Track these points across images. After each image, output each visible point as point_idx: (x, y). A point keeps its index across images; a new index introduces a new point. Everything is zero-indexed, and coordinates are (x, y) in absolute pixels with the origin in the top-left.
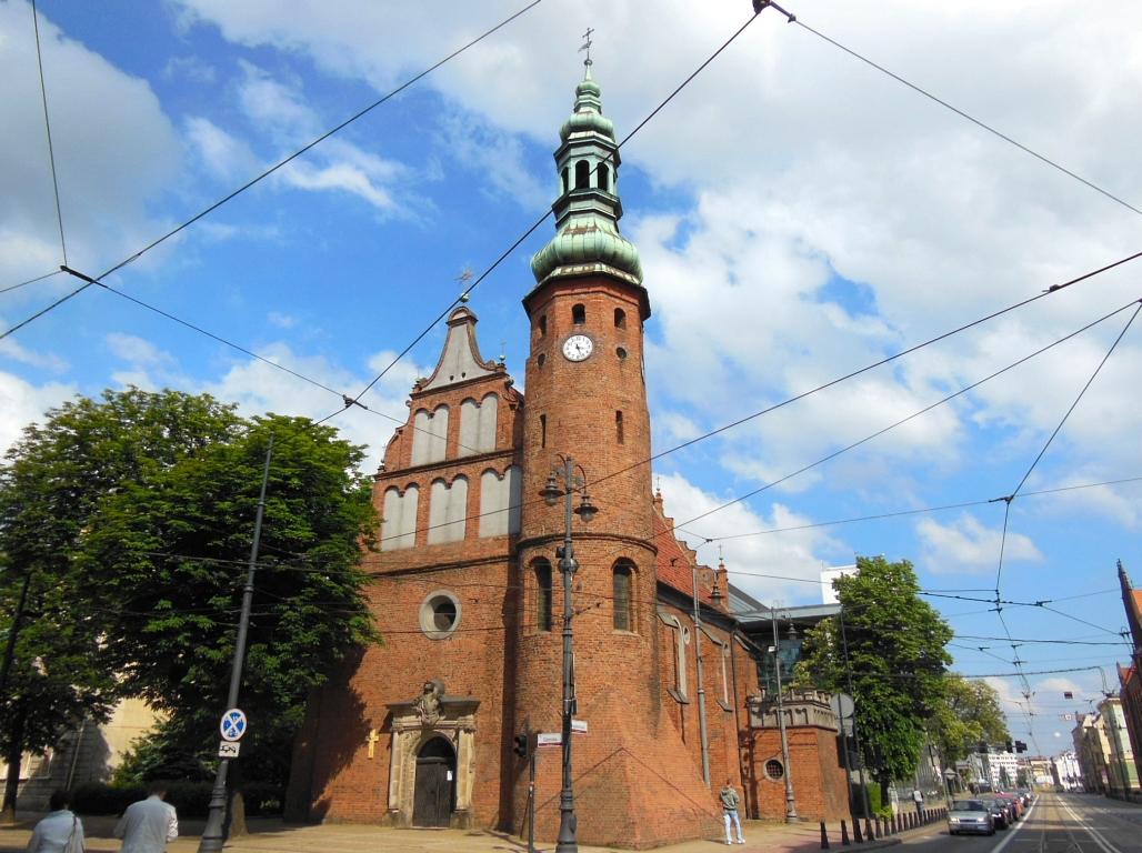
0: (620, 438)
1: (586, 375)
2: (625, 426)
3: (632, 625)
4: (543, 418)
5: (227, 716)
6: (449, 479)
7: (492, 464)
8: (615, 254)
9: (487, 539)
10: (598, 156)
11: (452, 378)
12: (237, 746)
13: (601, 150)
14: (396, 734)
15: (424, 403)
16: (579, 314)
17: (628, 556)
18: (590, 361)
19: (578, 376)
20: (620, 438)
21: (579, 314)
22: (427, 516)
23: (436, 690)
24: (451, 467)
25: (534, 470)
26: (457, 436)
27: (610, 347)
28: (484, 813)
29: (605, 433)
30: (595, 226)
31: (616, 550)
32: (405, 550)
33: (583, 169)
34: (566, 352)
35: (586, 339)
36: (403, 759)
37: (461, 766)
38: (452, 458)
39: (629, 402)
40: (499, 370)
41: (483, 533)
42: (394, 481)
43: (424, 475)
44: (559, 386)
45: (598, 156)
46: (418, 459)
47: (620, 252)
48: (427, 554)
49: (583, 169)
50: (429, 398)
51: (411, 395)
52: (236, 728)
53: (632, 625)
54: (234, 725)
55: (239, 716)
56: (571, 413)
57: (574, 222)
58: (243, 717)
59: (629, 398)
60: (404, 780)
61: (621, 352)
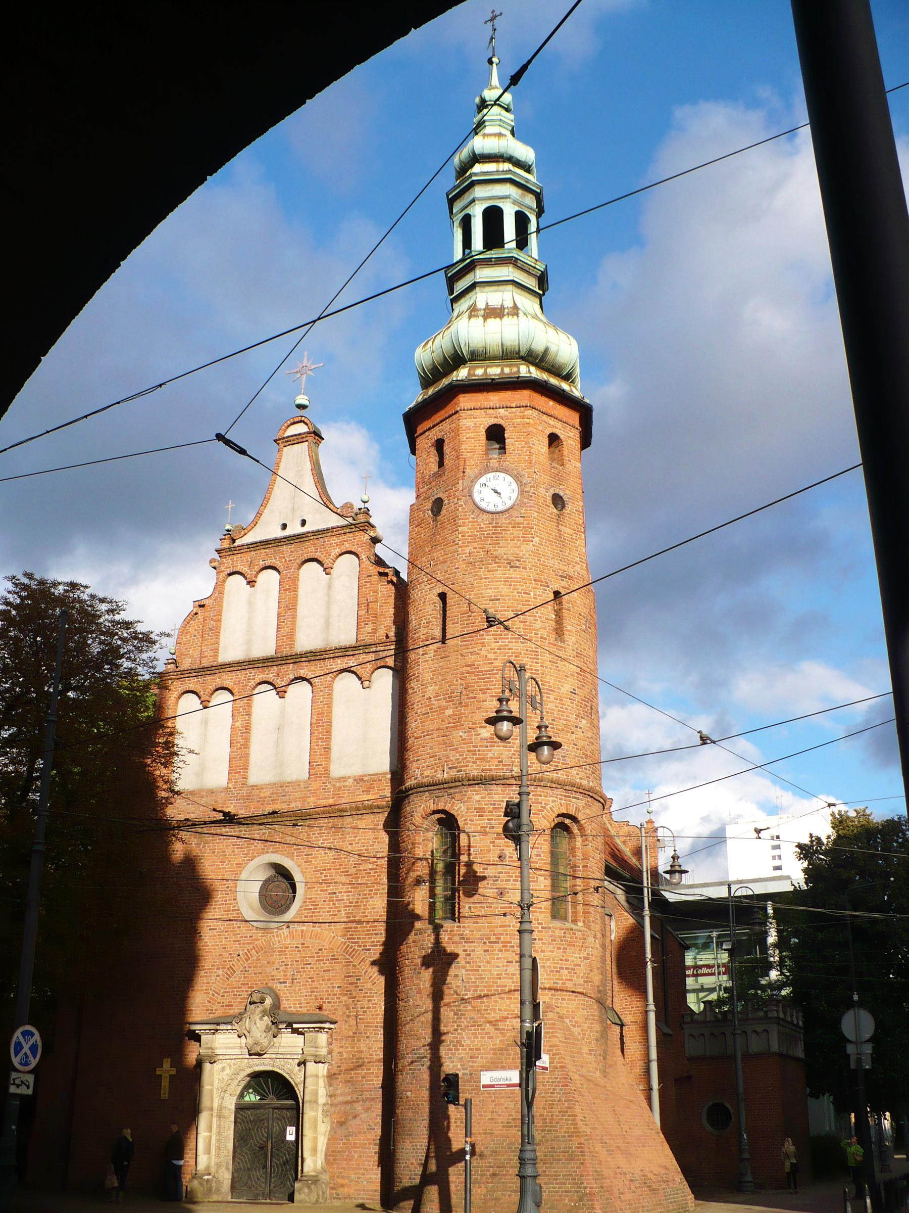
0: (559, 631)
2: (565, 613)
3: (575, 913)
4: (443, 596)
5: (18, 1034)
6: (279, 683)
8: (547, 350)
9: (343, 779)
10: (515, 202)
11: (284, 526)
13: (520, 191)
15: (240, 562)
16: (496, 434)
17: (572, 812)
18: (514, 513)
19: (496, 534)
22: (247, 740)
23: (268, 1001)
24: (285, 665)
25: (427, 677)
26: (294, 617)
28: (346, 1181)
29: (538, 625)
30: (515, 307)
32: (212, 792)
33: (493, 217)
34: (477, 497)
35: (509, 479)
37: (310, 1115)
38: (286, 651)
39: (570, 578)
40: (362, 519)
41: (336, 770)
42: (191, 684)
43: (241, 675)
44: (467, 550)
46: (230, 651)
47: (553, 349)
48: (248, 797)
49: (493, 217)
51: (218, 551)
52: (29, 1053)
53: (575, 913)
54: (26, 1049)
55: (32, 1035)
56: (490, 593)
57: (481, 298)
58: (37, 1037)
60: (219, 1133)
61: (558, 501)
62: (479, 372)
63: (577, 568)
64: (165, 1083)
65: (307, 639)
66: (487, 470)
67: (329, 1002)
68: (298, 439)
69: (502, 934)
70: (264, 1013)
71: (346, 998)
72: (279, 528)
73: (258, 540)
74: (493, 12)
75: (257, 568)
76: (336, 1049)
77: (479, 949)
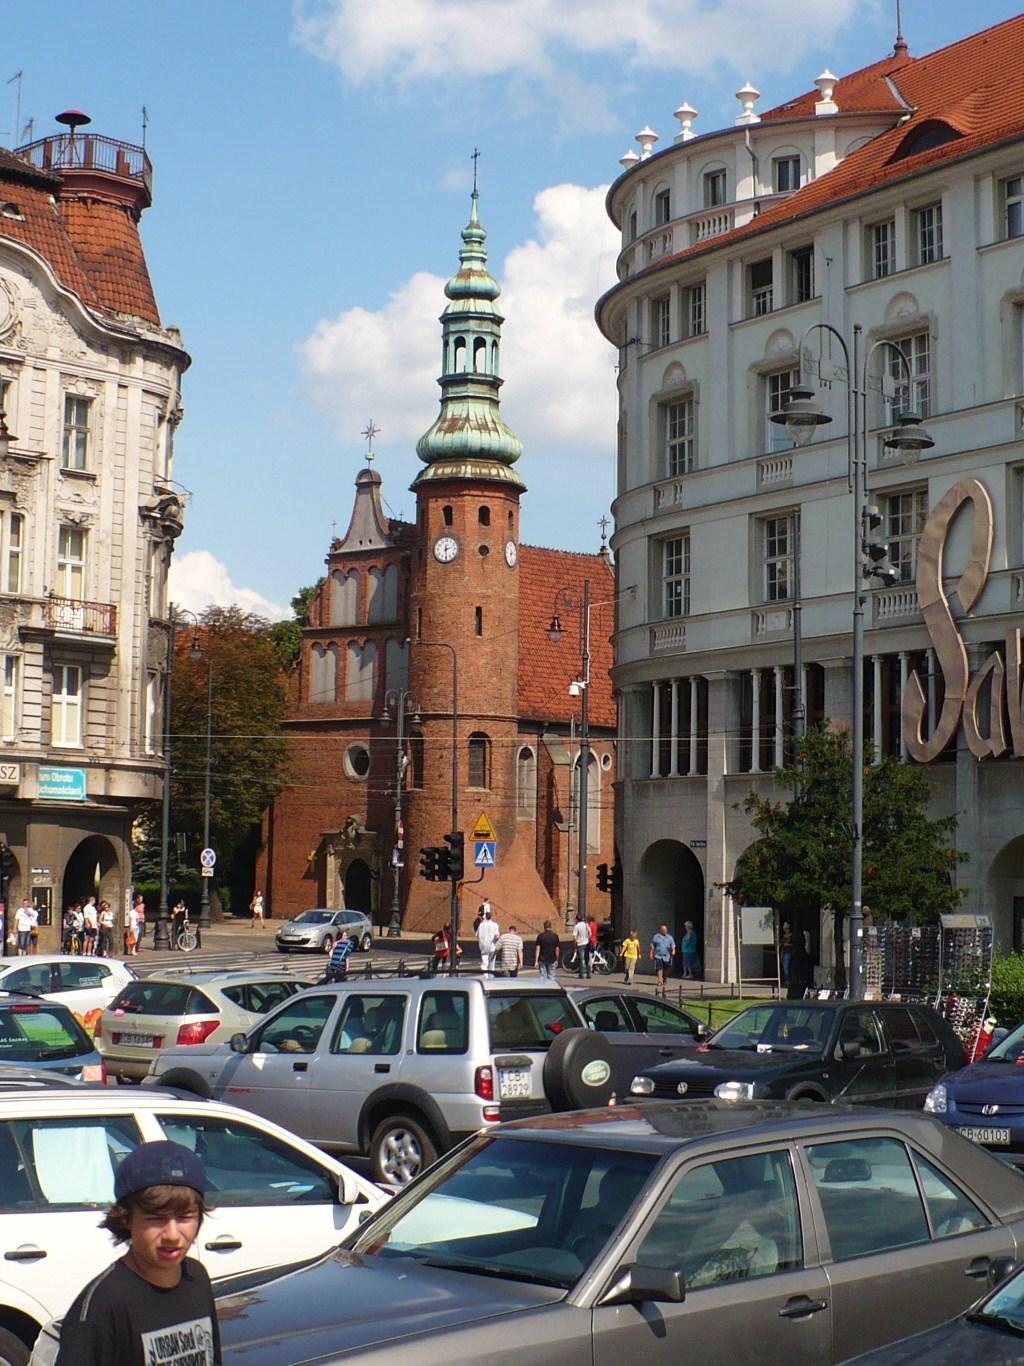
1: (452, 576)
4: (420, 610)
5: (204, 853)
7: (394, 634)
8: (482, 449)
13: (478, 322)
16: (448, 511)
20: (479, 632)
21: (448, 511)
27: (472, 547)
29: (465, 629)
31: (470, 727)
39: (488, 596)
45: (474, 332)
47: (486, 446)
54: (208, 858)
57: (454, 409)
58: (213, 853)
59: (490, 592)
61: (484, 550)
62: (440, 471)
63: (495, 588)
66: (442, 535)
73: (347, 550)
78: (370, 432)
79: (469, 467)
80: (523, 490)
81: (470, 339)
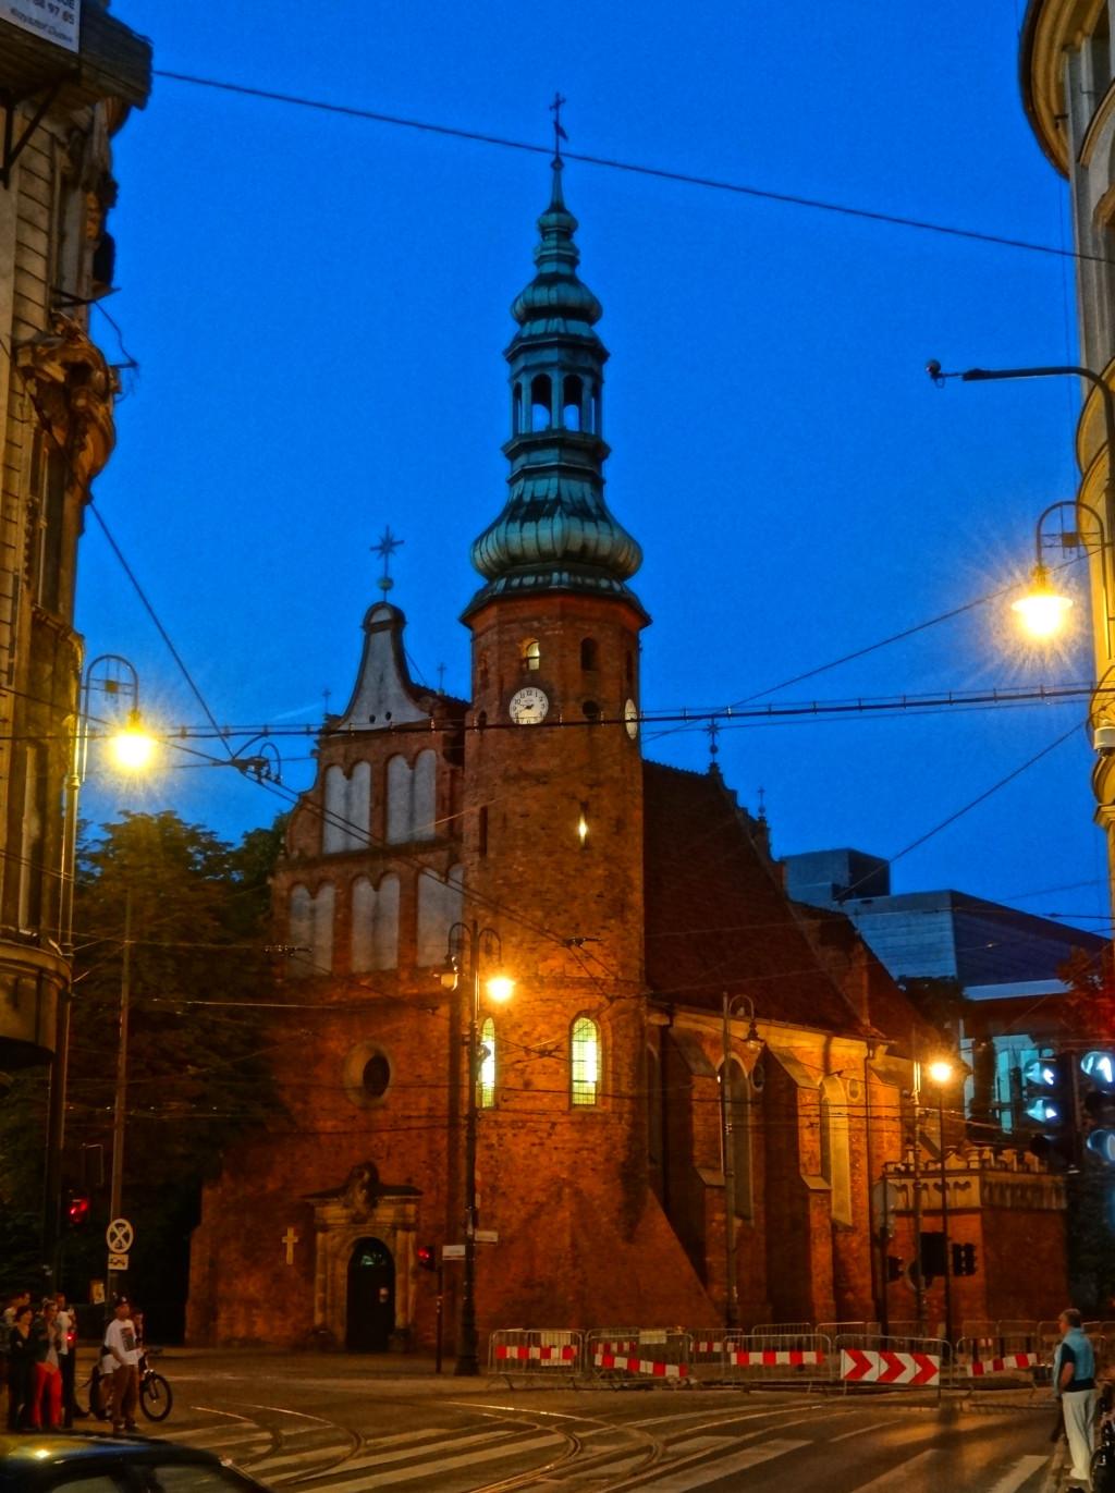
5: (112, 1227)
7: (431, 858)
8: (584, 547)
10: (563, 368)
11: (372, 719)
12: (126, 1258)
14: (320, 1236)
36: (329, 1266)
42: (302, 875)
46: (335, 841)
50: (341, 749)
52: (123, 1240)
54: (120, 1236)
55: (124, 1226)
56: (519, 809)
58: (128, 1227)
62: (516, 582)
64: (290, 1250)
65: (397, 832)
67: (417, 1176)
68: (382, 626)
69: (527, 1122)
70: (363, 1187)
71: (428, 1172)
72: (367, 720)
74: (557, 95)
75: (351, 761)
76: (423, 1218)
77: (510, 1134)
78: (387, 546)
79: (565, 576)
80: (646, 620)
81: (557, 380)
